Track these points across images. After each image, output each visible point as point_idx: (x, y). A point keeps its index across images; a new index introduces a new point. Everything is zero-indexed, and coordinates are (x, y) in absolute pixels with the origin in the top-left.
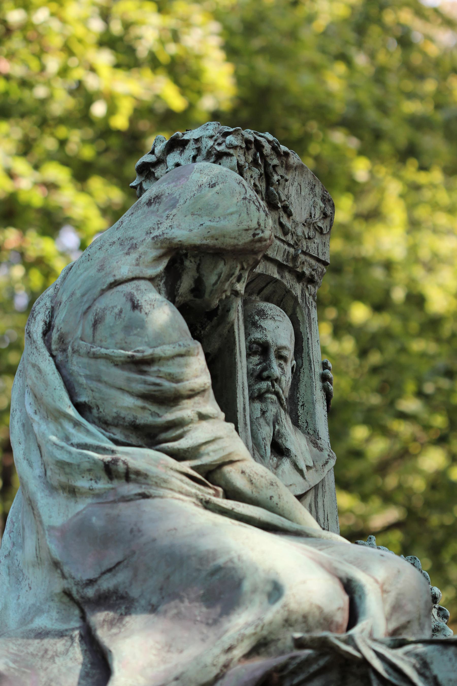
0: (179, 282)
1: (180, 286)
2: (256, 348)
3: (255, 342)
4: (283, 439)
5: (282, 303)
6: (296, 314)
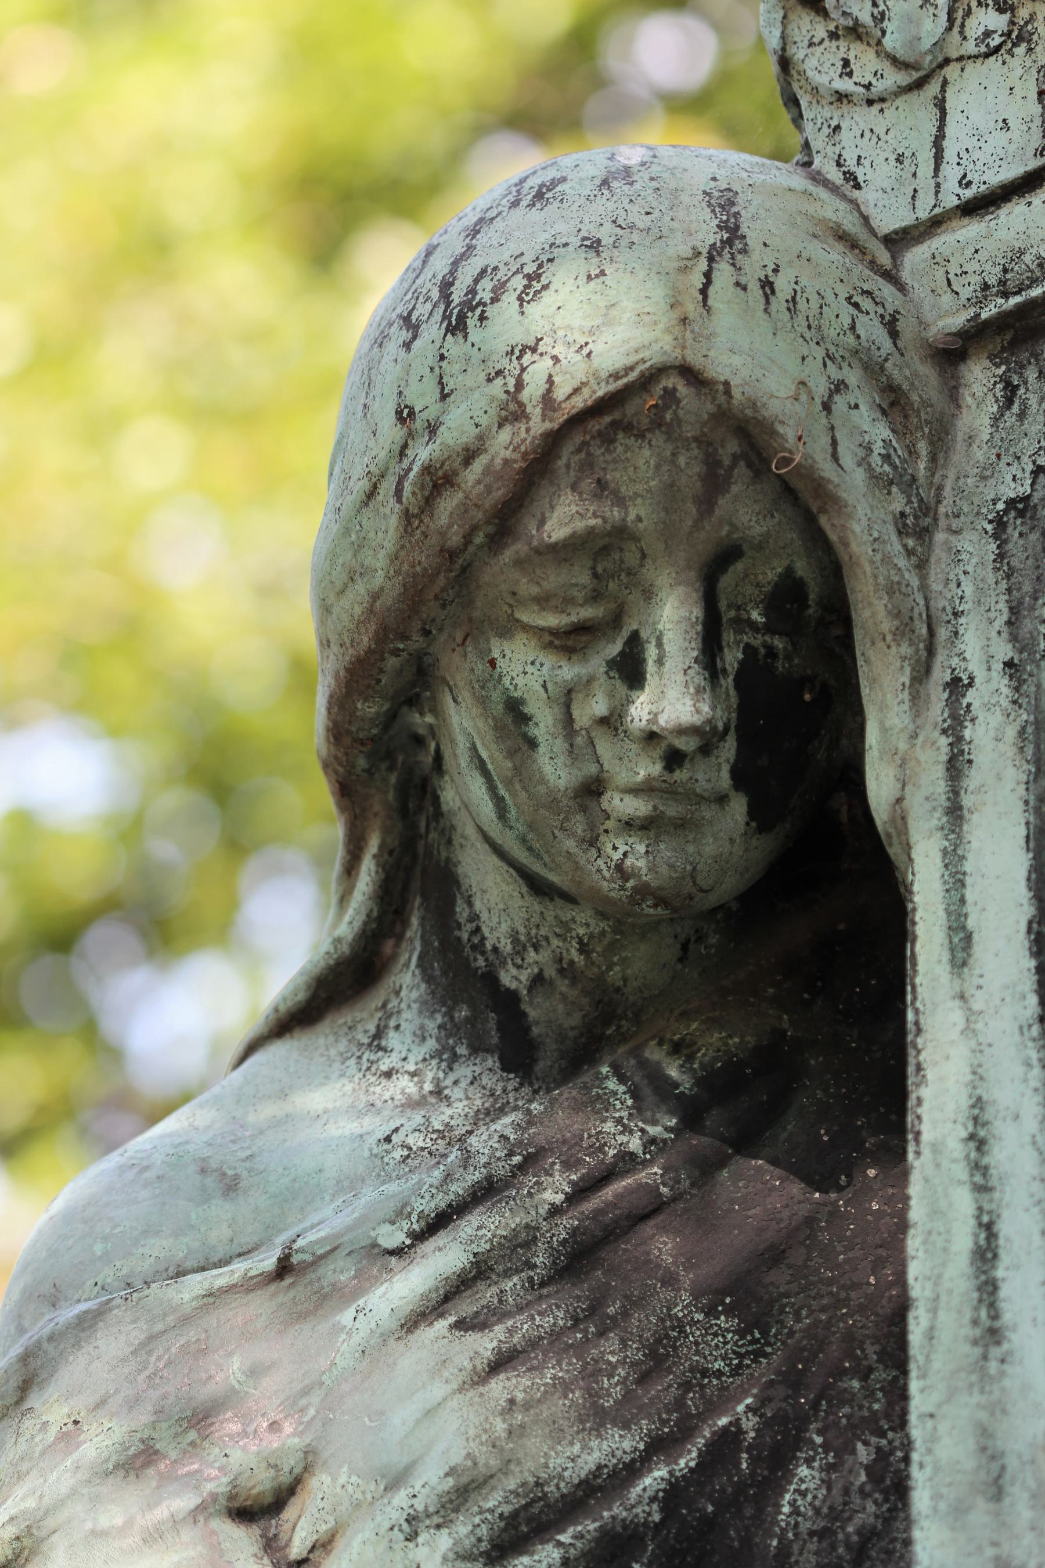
0: (461, 911)
1: (474, 917)
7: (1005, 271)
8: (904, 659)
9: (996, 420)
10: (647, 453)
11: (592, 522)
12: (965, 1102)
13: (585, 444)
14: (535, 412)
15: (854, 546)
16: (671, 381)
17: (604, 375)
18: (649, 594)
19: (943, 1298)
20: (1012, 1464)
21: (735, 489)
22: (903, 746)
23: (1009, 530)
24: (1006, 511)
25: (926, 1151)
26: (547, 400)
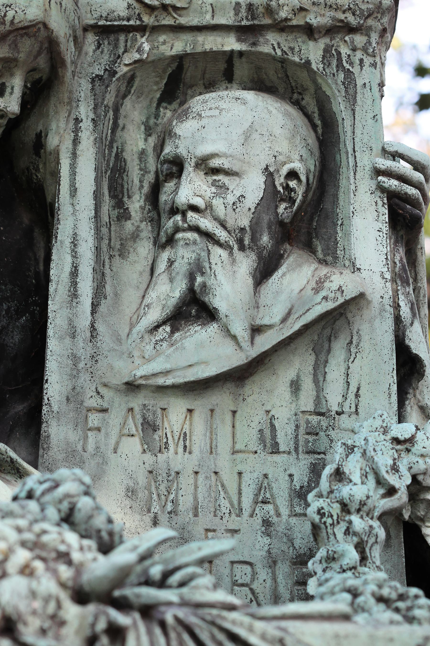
2: (167, 170)
3: (166, 161)
4: (211, 295)
5: (290, 79)
6: (321, 88)
7: (108, 14)
8: (67, 110)
9: (94, 51)
10: (29, 42)
11: (10, 55)
12: (71, 233)
13: (17, 36)
14: (8, 24)
15: (65, 79)
16: (41, 26)
17: (28, 20)
18: (12, 75)
19: (60, 282)
20: (78, 330)
21: (42, 55)
22: (62, 132)
23: (96, 83)
24: (95, 77)
25: (59, 242)
26: (12, 22)
